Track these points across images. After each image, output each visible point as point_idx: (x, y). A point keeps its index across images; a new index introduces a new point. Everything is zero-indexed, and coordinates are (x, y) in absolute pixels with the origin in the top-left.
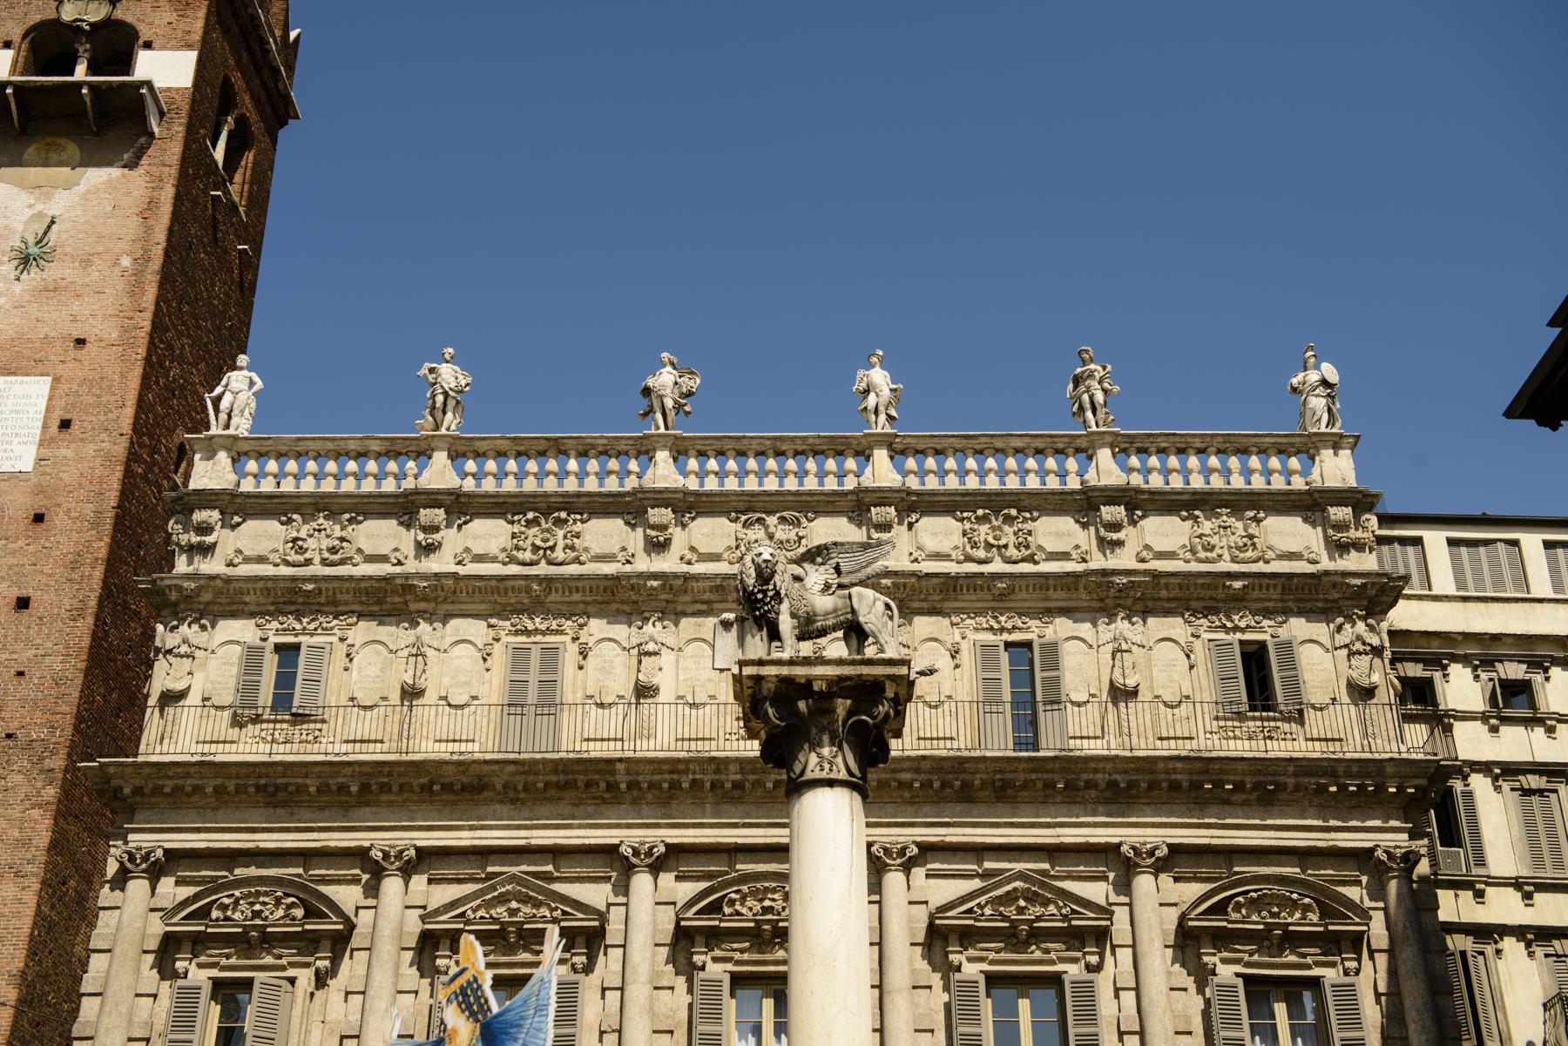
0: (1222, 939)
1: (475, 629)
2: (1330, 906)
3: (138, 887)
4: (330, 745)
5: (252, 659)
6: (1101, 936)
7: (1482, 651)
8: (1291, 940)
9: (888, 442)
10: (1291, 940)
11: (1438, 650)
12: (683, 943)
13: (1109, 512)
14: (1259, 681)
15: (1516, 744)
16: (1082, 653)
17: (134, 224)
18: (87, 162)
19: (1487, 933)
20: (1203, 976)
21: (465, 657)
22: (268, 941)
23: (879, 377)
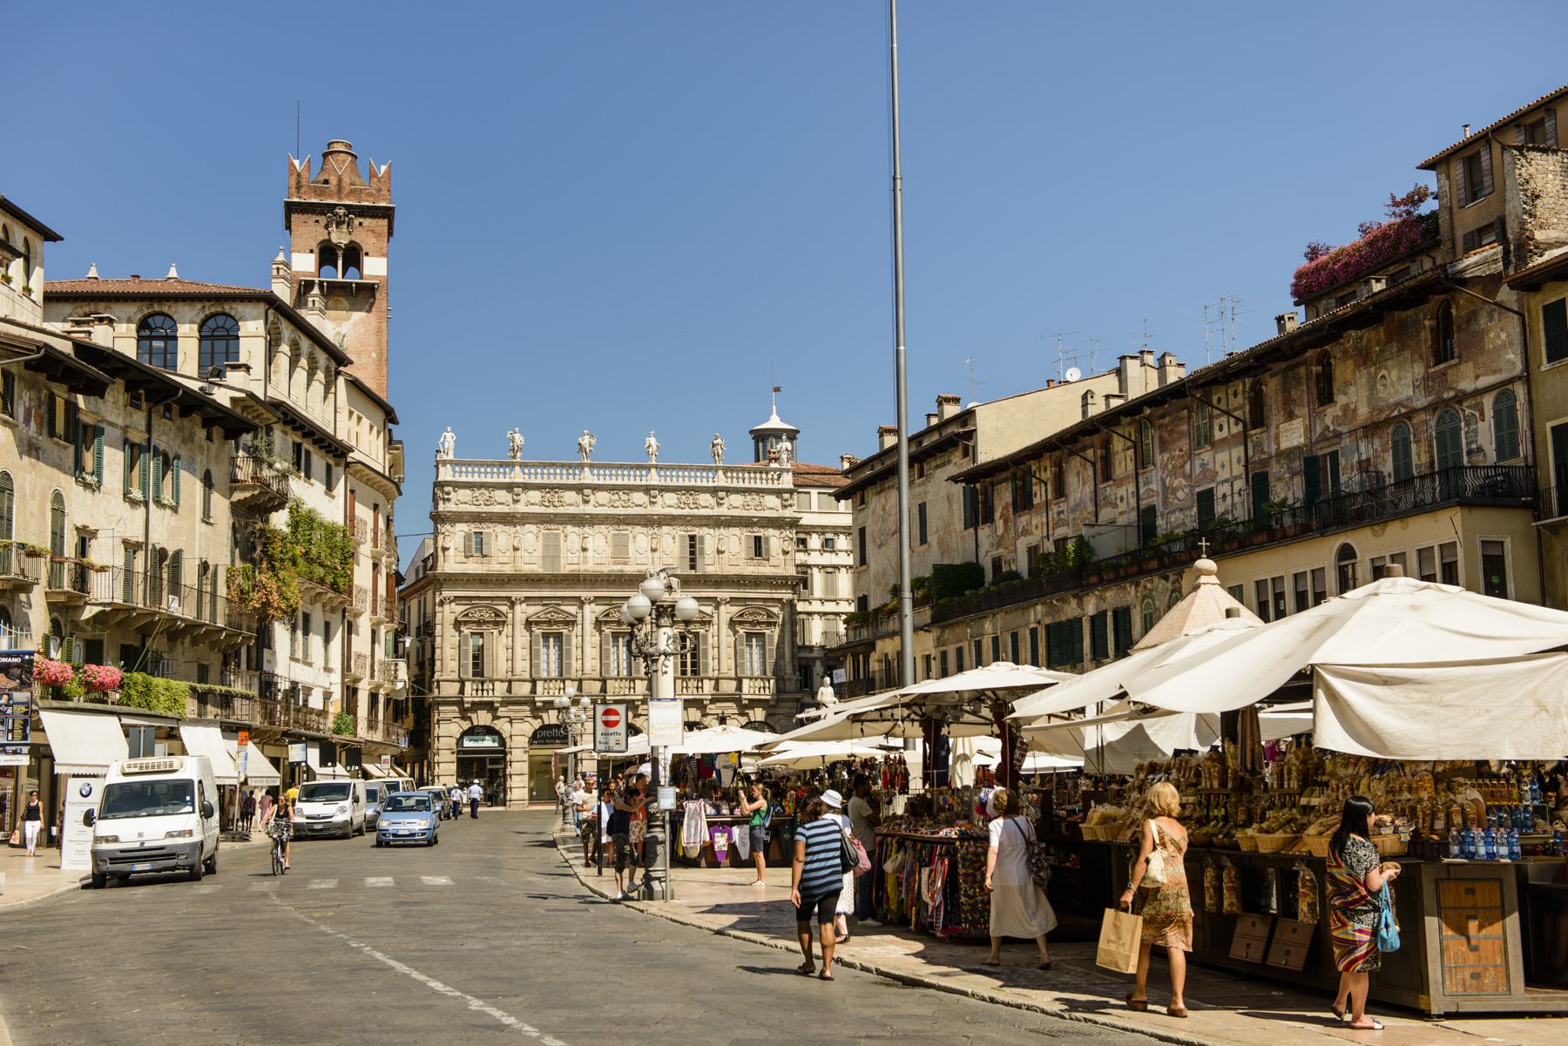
0: (741, 623)
1: (533, 528)
2: (770, 614)
3: (446, 607)
4: (493, 567)
5: (467, 537)
6: (710, 622)
7: (821, 530)
8: (759, 623)
9: (656, 467)
10: (759, 623)
11: (810, 530)
12: (598, 624)
13: (721, 494)
14: (759, 547)
15: (828, 559)
16: (710, 538)
17: (374, 337)
18: (351, 310)
19: (810, 614)
20: (735, 632)
21: (530, 537)
22: (485, 622)
23: (653, 441)
